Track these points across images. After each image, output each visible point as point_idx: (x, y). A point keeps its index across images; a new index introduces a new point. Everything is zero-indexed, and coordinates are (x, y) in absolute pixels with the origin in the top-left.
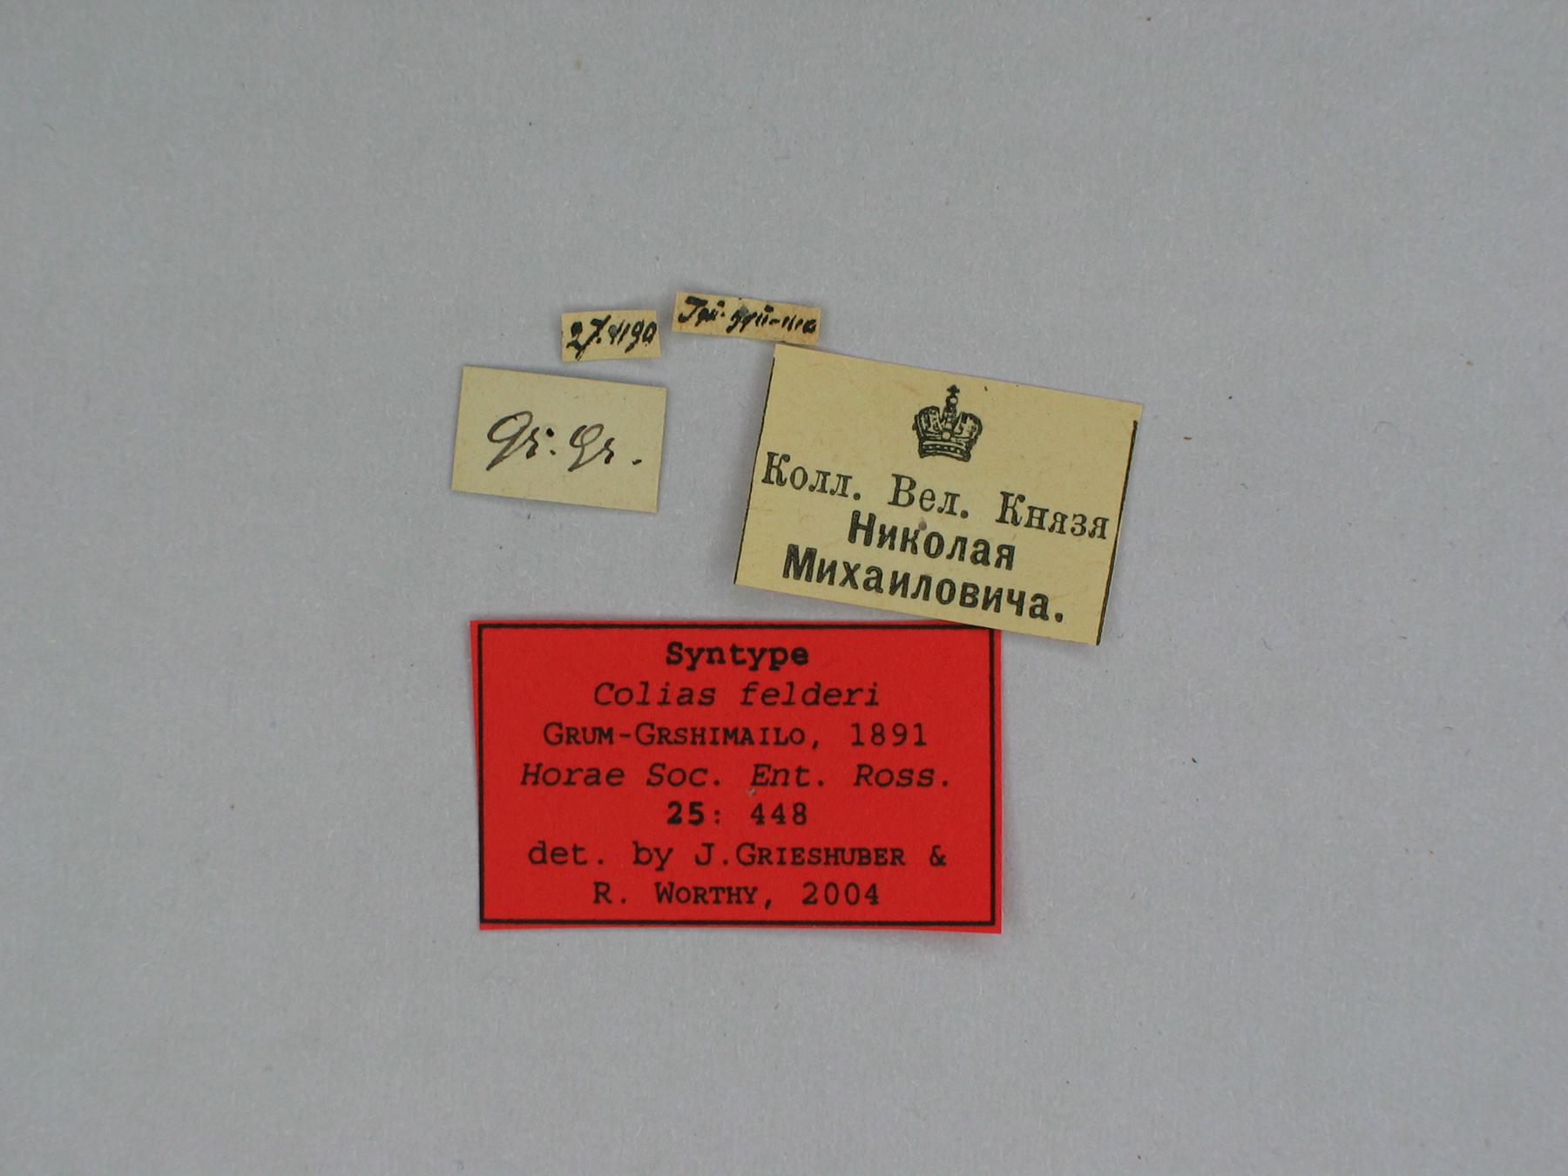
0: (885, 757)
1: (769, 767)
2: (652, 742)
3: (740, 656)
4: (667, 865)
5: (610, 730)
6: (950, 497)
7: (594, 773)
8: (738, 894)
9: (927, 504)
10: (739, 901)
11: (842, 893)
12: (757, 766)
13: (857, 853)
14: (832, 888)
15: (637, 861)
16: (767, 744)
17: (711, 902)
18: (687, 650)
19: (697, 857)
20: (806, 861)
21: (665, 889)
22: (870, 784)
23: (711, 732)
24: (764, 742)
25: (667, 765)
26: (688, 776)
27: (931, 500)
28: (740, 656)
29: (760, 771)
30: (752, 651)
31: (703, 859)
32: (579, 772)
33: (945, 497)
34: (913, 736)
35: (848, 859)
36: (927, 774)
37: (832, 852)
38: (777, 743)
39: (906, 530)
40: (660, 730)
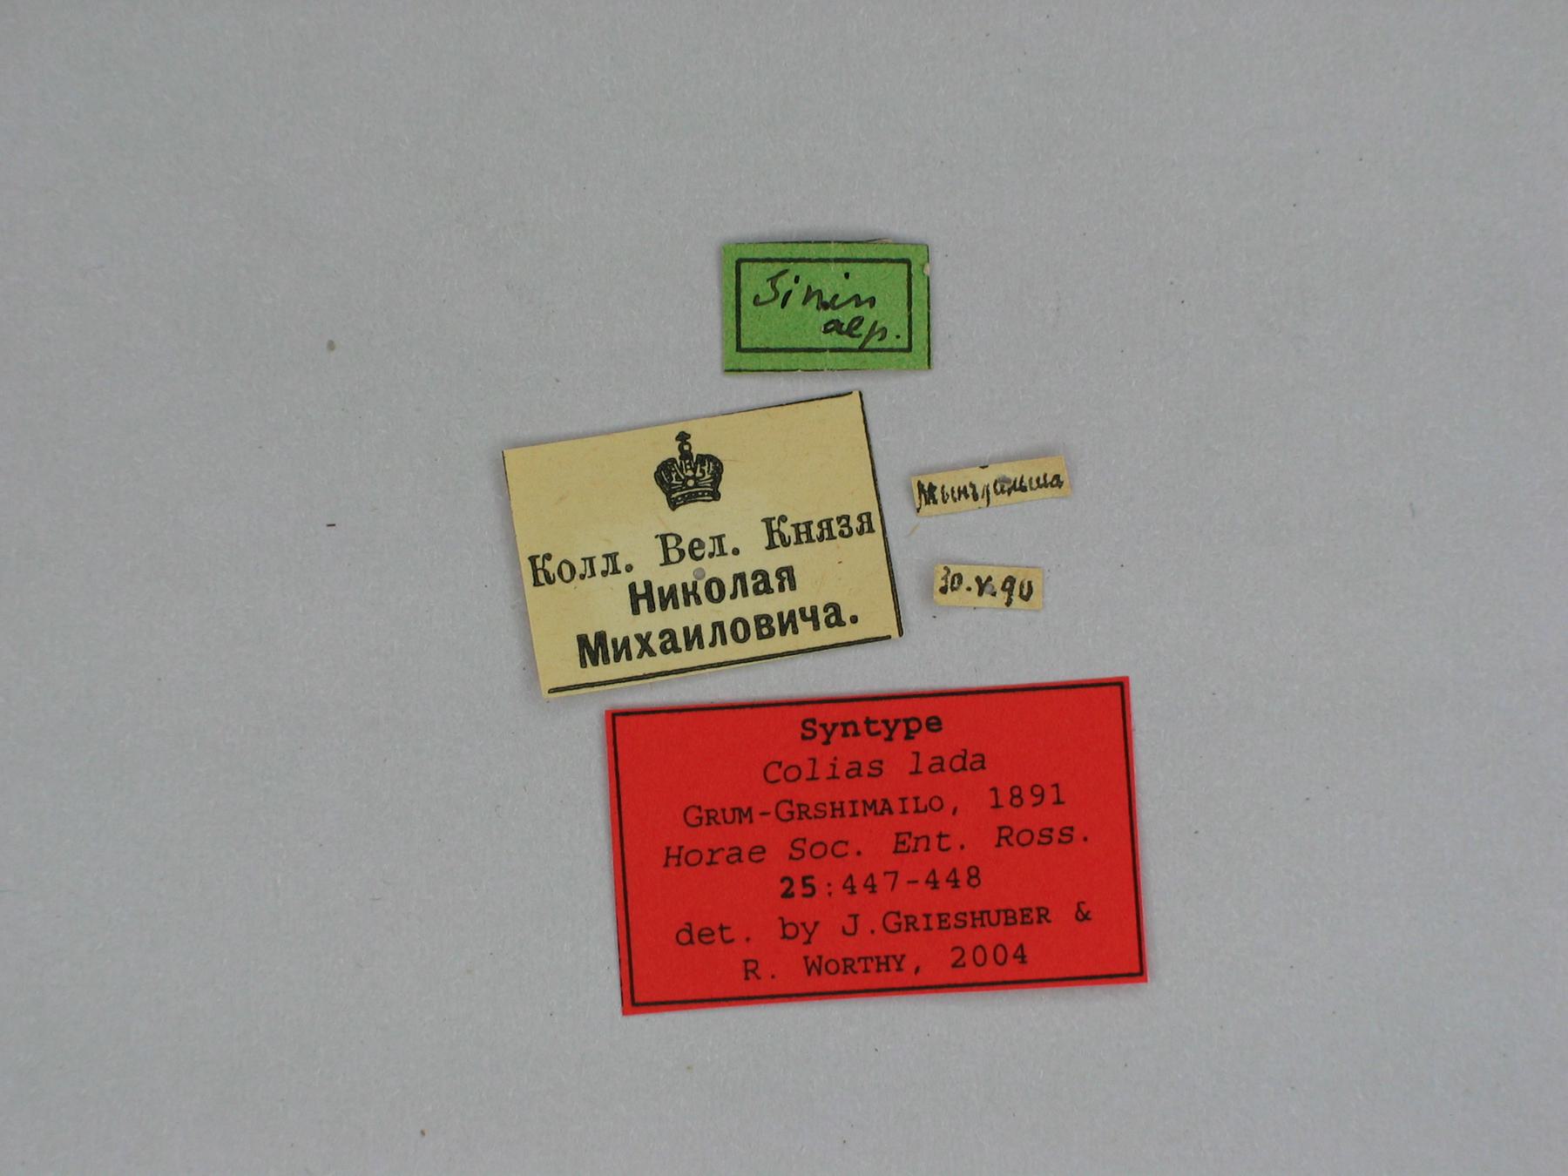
0: (1026, 818)
2: (792, 818)
3: (873, 728)
5: (750, 809)
6: (716, 540)
7: (737, 851)
8: (887, 963)
9: (698, 553)
12: (898, 835)
13: (1002, 914)
14: (980, 950)
15: (784, 936)
16: (907, 812)
18: (821, 725)
19: (843, 928)
20: (952, 926)
21: (813, 963)
24: (904, 812)
28: (873, 728)
29: (901, 838)
30: (886, 722)
31: (850, 929)
32: (721, 852)
33: (712, 541)
35: (994, 919)
37: (977, 915)
38: (917, 811)
40: (799, 806)
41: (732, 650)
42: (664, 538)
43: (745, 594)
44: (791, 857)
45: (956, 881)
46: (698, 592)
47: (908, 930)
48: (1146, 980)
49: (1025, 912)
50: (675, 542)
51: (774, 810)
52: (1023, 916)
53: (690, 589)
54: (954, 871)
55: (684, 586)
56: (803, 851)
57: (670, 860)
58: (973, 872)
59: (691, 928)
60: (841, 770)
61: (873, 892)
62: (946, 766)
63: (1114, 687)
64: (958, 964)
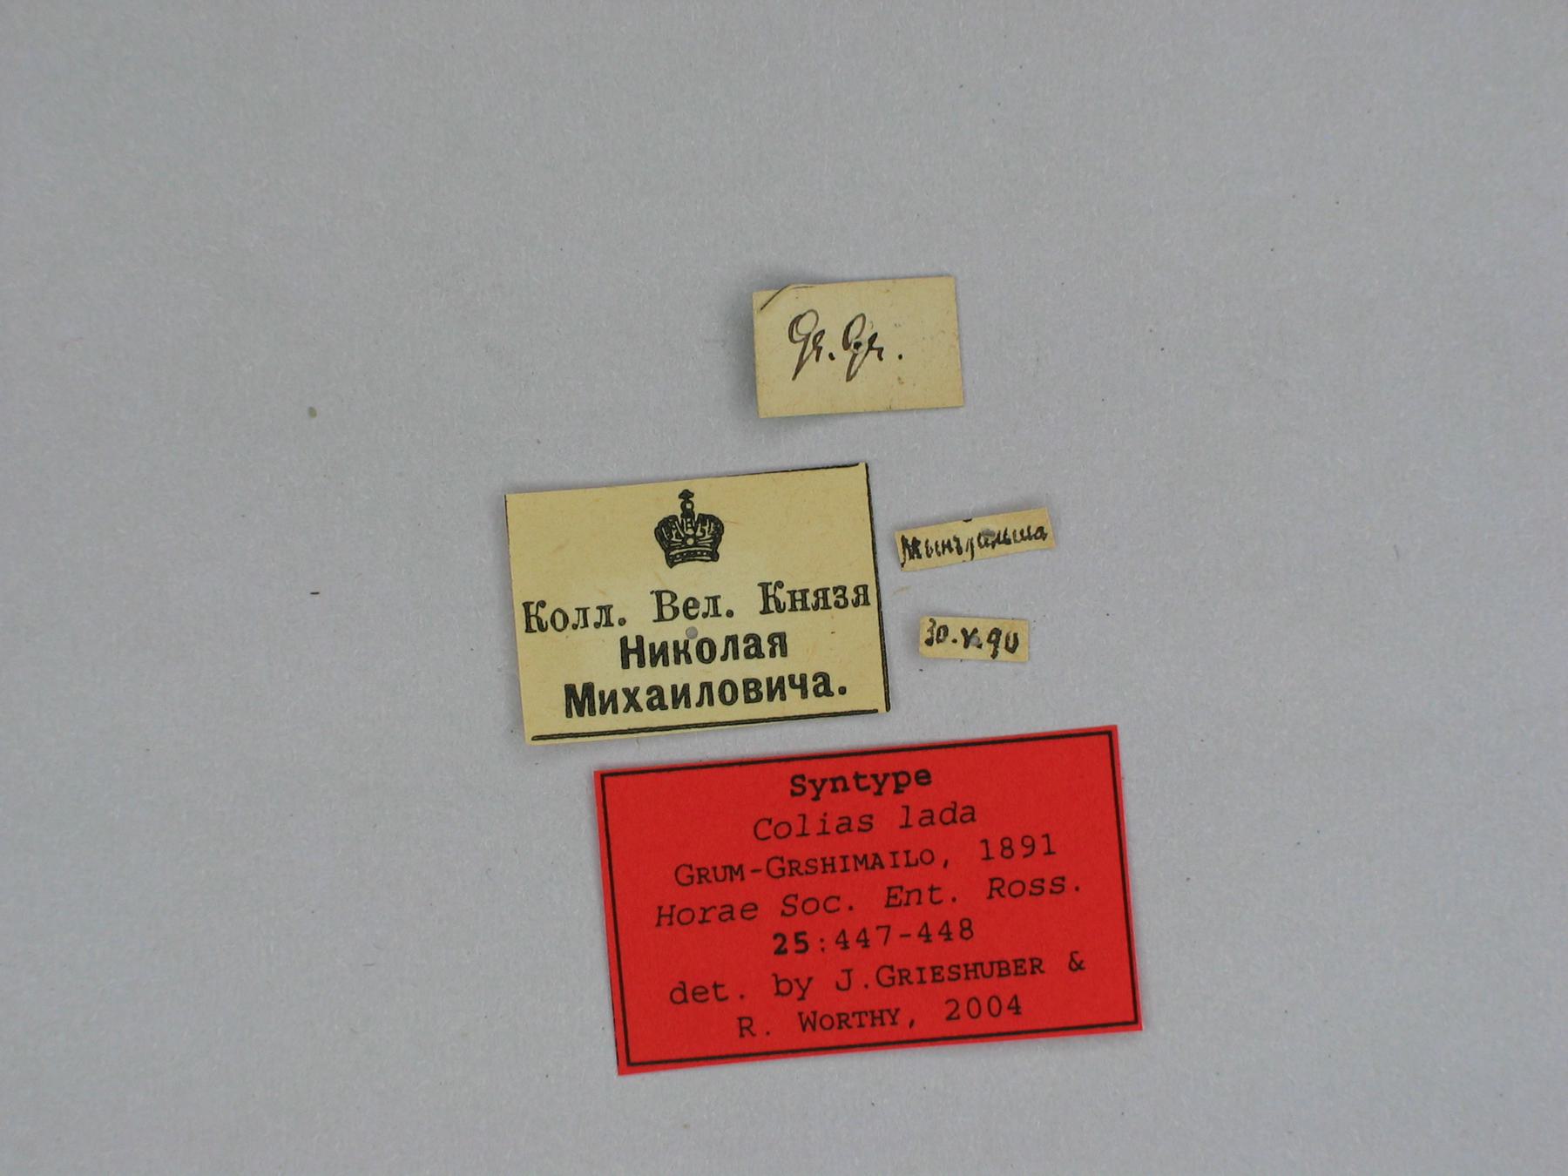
1: (901, 888)
2: (784, 875)
3: (862, 783)
4: (805, 996)
5: (741, 867)
6: (711, 600)
7: (729, 909)
8: (881, 1018)
9: (692, 612)
10: (882, 1024)
11: (984, 1003)
12: (889, 889)
13: (995, 965)
15: (778, 993)
17: (855, 1027)
20: (946, 977)
21: (808, 1019)
22: (1000, 895)
25: (799, 897)
28: (862, 783)
29: (893, 892)
30: (875, 776)
31: (844, 984)
32: (713, 909)
33: (707, 601)
34: (1041, 846)
36: (1060, 881)
37: (971, 967)
38: (908, 864)
39: (676, 644)
42: (659, 594)
44: (783, 913)
45: (948, 934)
46: (689, 651)
47: (901, 983)
48: (1141, 1029)
49: (1019, 963)
51: (765, 867)
52: (1016, 967)
53: (681, 647)
54: (947, 923)
55: (676, 644)
56: (795, 907)
57: (663, 919)
58: (965, 924)
59: (684, 985)
60: (831, 826)
61: (866, 946)
62: (936, 819)
63: (1102, 736)
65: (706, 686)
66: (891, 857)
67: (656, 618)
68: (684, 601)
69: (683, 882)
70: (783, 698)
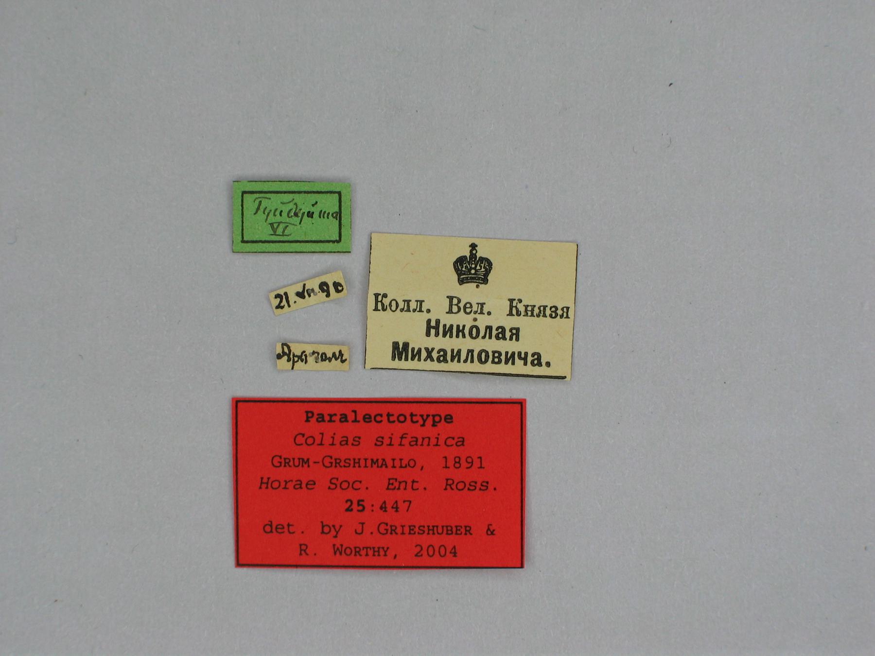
1: (396, 480)
4: (338, 536)
6: (480, 305)
7: (299, 482)
8: (379, 551)
9: (468, 310)
10: (379, 555)
11: (437, 549)
12: (389, 479)
13: (445, 528)
14: (431, 547)
15: (323, 532)
19: (356, 530)
20: (417, 533)
21: (338, 549)
23: (364, 461)
24: (394, 467)
25: (339, 479)
26: (351, 484)
27: (470, 308)
29: (391, 481)
31: (359, 531)
34: (477, 463)
35: (440, 531)
36: (484, 484)
37: (431, 528)
38: (401, 467)
41: (476, 367)
42: (451, 298)
43: (490, 337)
49: (458, 528)
50: (457, 302)
52: (457, 530)
53: (461, 328)
55: (458, 326)
57: (263, 485)
59: (271, 523)
64: (419, 555)
65: (471, 351)
66: (392, 461)
67: (448, 311)
68: (465, 303)
69: (275, 464)
70: (513, 363)
